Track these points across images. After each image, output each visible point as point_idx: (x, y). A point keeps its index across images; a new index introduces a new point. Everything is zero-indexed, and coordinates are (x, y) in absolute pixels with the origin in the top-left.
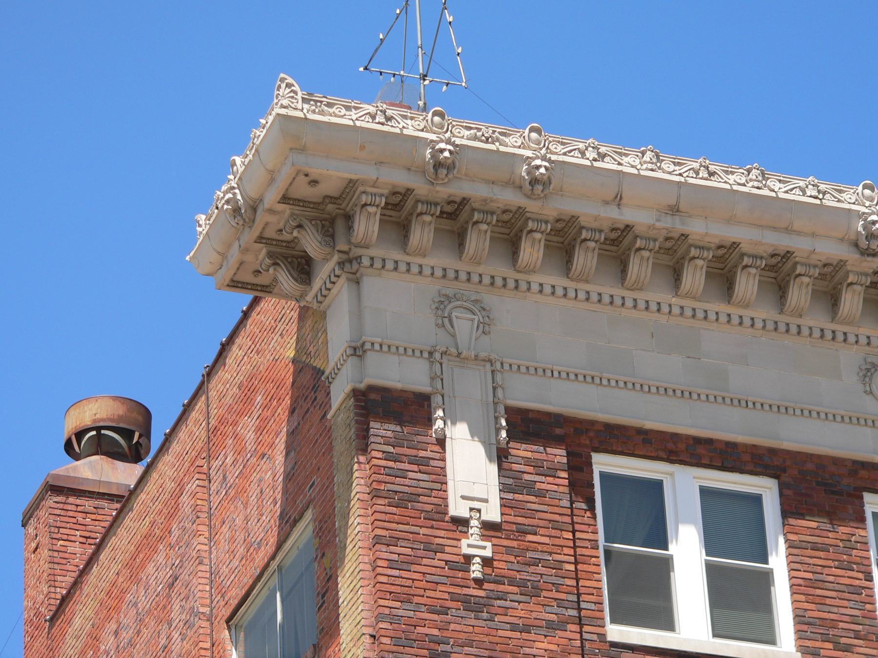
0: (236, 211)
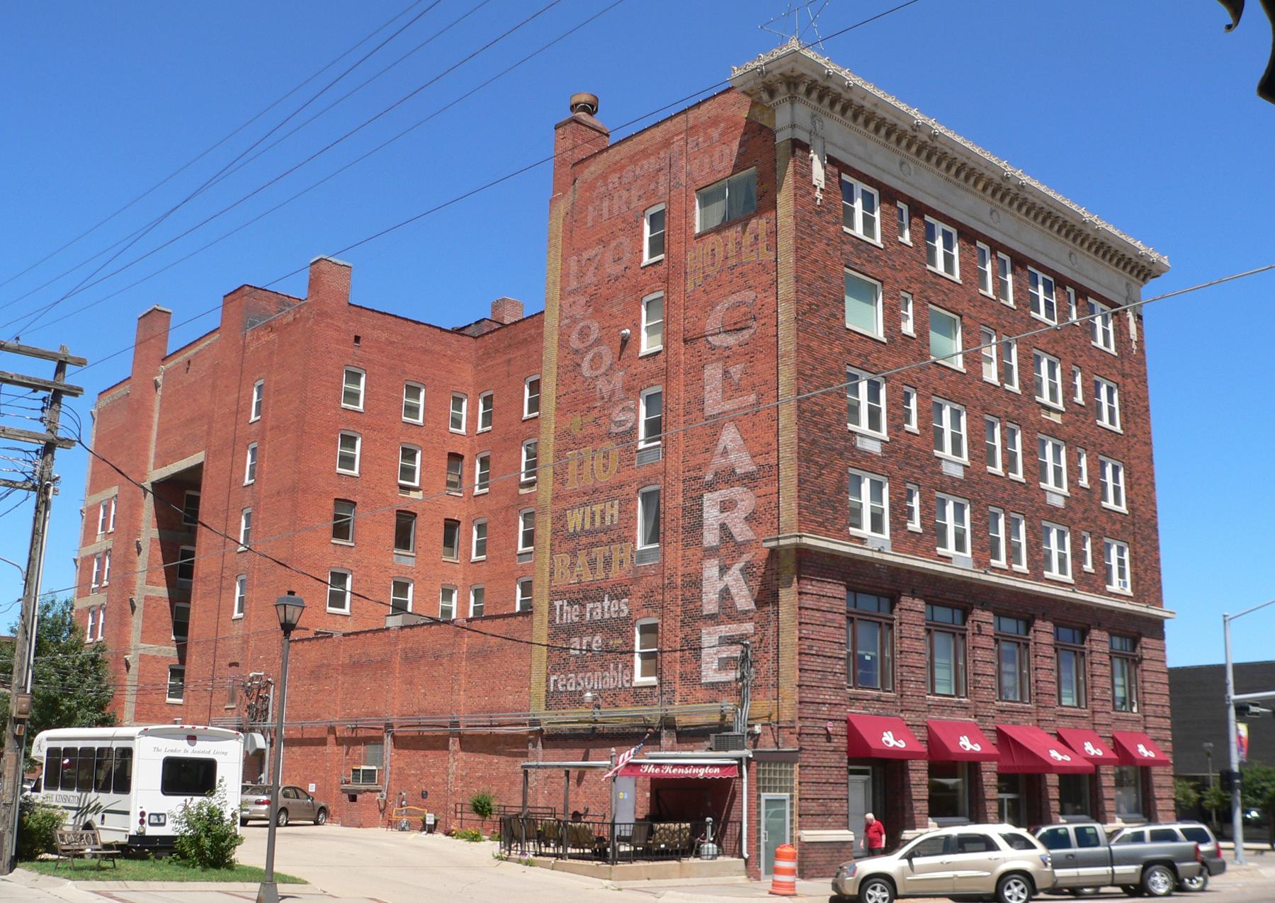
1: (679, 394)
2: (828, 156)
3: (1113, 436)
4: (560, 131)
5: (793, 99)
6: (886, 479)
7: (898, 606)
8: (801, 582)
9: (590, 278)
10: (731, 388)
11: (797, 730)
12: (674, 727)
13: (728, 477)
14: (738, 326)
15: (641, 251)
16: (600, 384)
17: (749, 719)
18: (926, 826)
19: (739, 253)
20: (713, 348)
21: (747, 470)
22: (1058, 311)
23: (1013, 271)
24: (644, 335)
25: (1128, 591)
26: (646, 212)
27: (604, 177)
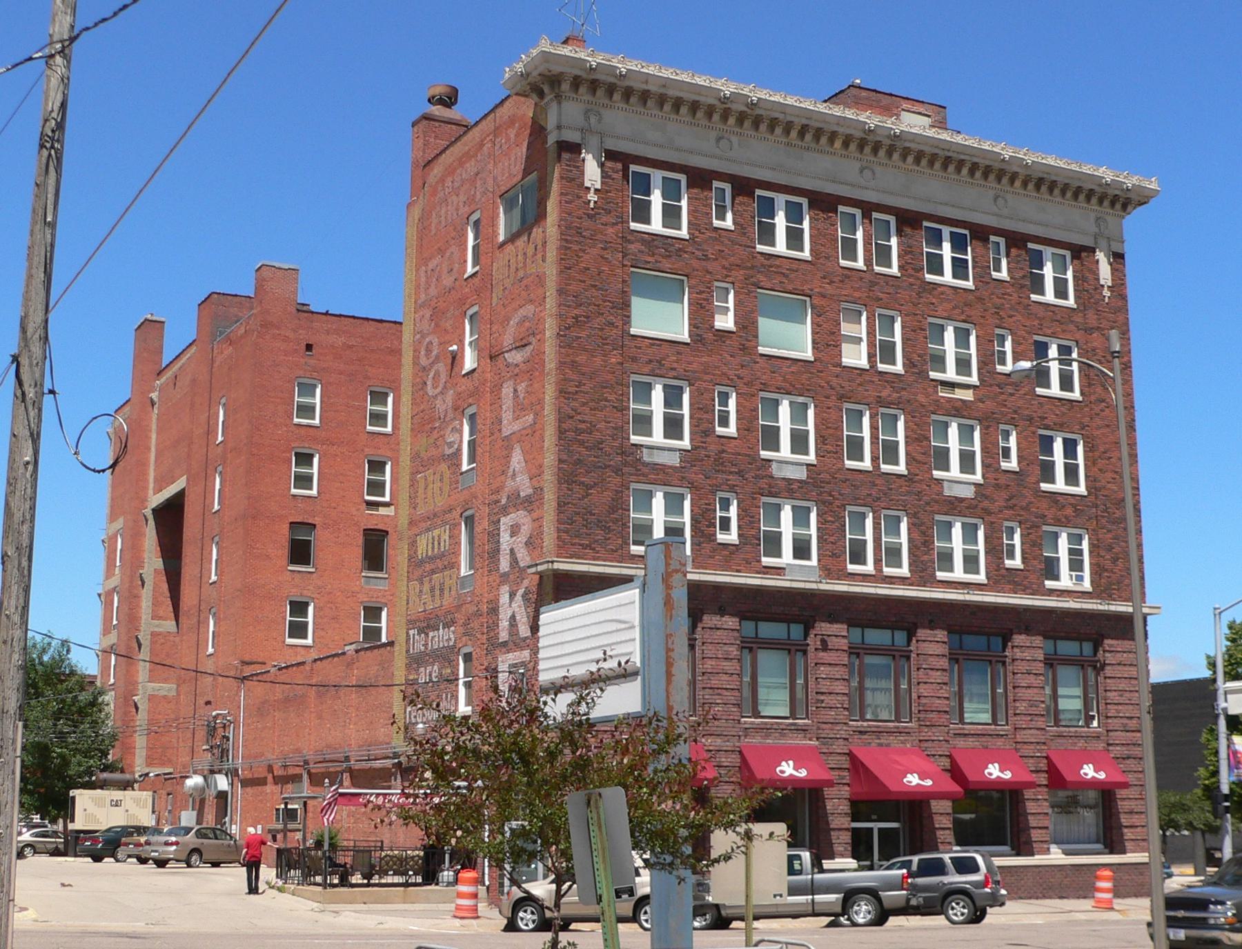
0: (522, 75)
3: (1063, 405)
4: (416, 129)
5: (558, 97)
7: (700, 625)
9: (433, 291)
15: (465, 261)
22: (974, 268)
23: (900, 233)
26: (471, 218)
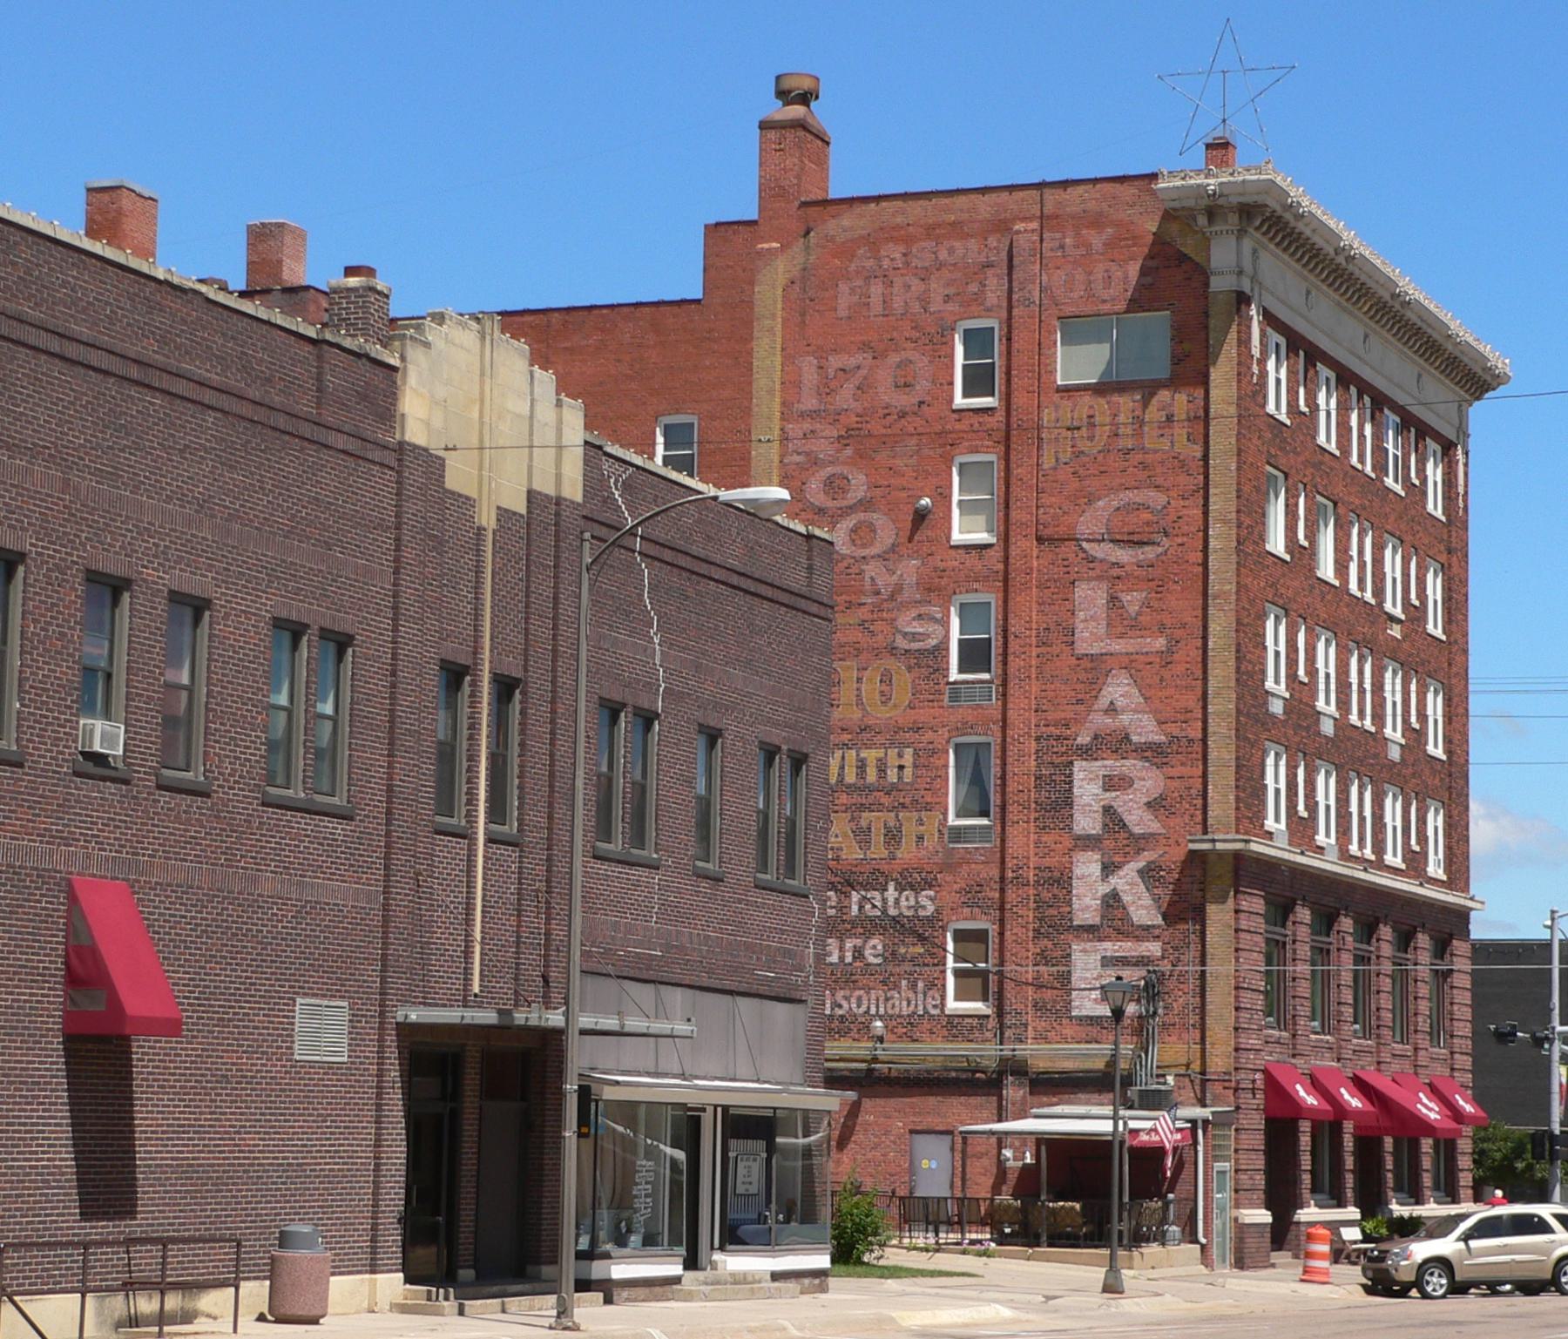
0: (1215, 194)
1: (1029, 613)
2: (1264, 309)
4: (772, 135)
5: (1241, 233)
6: (1283, 748)
7: (1291, 918)
8: (1240, 896)
10: (1119, 620)
11: (1233, 1084)
12: (1026, 1073)
13: (1119, 744)
14: (1135, 538)
15: (951, 383)
16: (871, 570)
17: (1158, 1067)
18: (1309, 1206)
19: (1138, 434)
20: (1092, 560)
21: (1150, 739)
24: (956, 512)
25: (1441, 874)
26: (959, 323)
27: (873, 242)
